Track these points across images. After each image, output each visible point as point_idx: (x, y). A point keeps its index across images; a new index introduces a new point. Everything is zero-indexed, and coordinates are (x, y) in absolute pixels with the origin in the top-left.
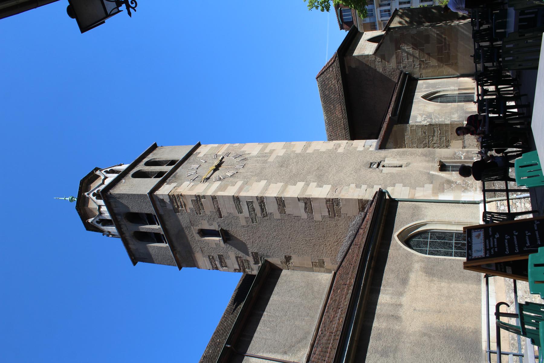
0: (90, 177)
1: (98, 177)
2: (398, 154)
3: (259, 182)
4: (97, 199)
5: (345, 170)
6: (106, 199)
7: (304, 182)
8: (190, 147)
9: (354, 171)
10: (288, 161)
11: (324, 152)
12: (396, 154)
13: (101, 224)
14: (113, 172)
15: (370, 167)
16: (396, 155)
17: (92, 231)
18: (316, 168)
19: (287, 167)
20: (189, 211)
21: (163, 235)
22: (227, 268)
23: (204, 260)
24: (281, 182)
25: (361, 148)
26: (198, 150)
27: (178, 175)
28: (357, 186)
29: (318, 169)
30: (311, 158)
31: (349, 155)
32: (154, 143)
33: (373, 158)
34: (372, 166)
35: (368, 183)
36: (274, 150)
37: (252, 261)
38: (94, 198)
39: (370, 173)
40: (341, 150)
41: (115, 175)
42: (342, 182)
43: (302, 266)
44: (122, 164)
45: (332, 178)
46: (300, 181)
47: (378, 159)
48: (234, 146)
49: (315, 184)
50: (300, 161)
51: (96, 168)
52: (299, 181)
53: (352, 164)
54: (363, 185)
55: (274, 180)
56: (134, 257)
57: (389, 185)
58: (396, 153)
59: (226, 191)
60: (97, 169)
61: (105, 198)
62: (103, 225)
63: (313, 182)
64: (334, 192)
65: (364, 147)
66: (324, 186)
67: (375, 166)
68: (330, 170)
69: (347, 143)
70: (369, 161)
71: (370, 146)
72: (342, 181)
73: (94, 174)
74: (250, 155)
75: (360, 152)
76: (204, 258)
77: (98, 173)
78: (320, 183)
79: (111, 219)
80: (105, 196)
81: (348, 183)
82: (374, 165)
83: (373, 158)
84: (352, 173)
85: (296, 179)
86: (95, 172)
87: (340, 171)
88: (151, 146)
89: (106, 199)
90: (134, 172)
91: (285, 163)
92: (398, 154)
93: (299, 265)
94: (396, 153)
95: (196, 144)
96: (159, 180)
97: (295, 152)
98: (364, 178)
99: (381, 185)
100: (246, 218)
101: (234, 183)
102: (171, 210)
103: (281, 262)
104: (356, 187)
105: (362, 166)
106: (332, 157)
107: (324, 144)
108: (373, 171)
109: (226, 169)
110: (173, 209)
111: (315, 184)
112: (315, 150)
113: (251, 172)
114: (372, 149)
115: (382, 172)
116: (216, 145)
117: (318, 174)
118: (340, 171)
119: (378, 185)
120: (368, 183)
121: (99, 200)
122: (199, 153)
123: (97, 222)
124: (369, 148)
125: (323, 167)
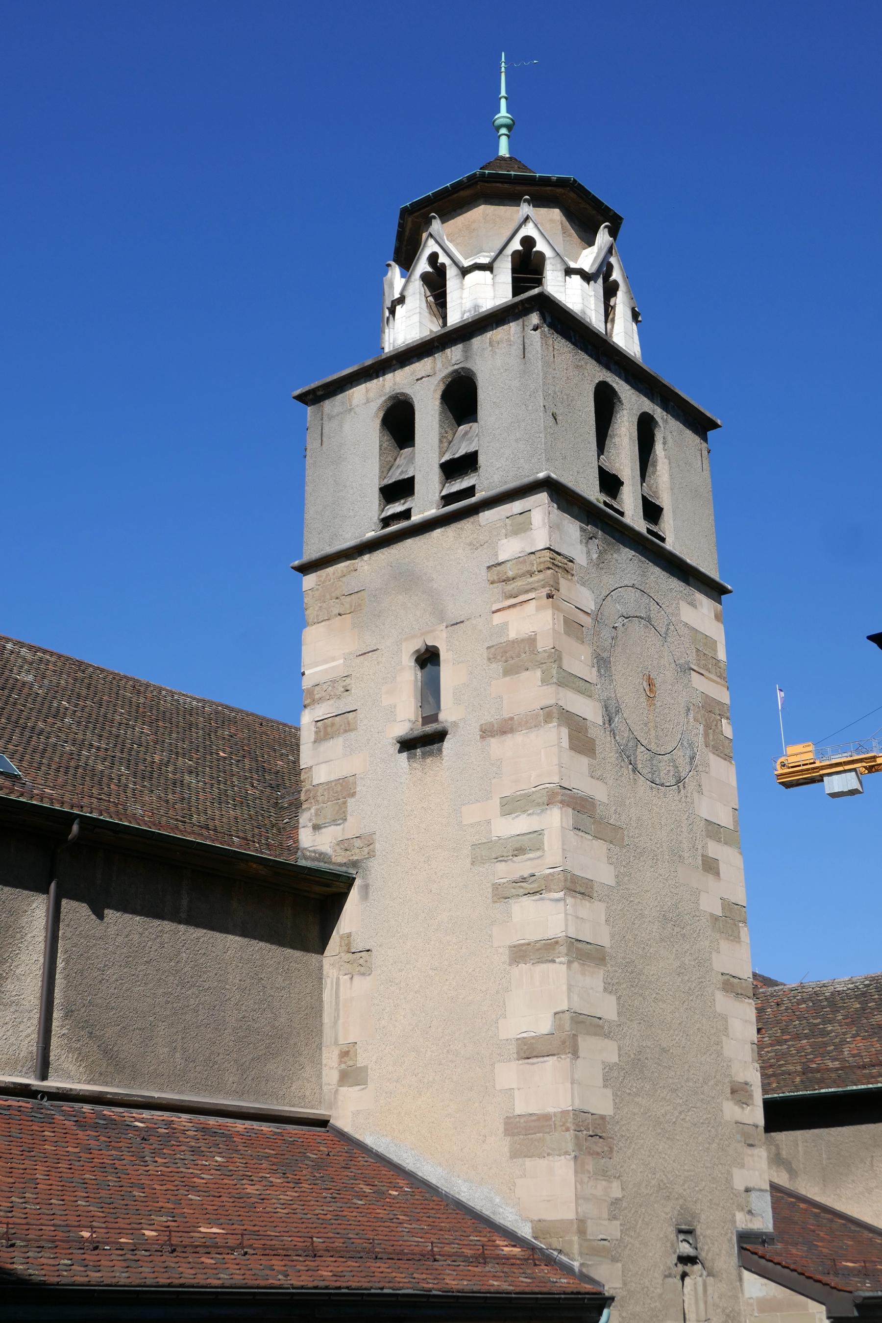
0: (587, 206)
1: (588, 238)
2: (728, 1316)
3: (609, 858)
4: (515, 254)
5: (667, 1146)
6: (517, 311)
7: (616, 1019)
8: (710, 568)
9: (662, 1181)
10: (684, 936)
11: (719, 1054)
12: (727, 1311)
13: (429, 269)
14: (610, 291)
15: (680, 1231)
16: (723, 1311)
17: (401, 226)
18: (664, 1045)
19: (662, 940)
20: (498, 619)
21: (406, 514)
22: (313, 740)
23: (333, 659)
24: (613, 936)
25: (740, 1179)
26: (701, 598)
27: (615, 556)
28: (616, 1202)
29: (664, 1050)
30: (697, 1016)
31: (714, 1145)
32: (719, 422)
33: (709, 1232)
34: (681, 1237)
35: (627, 1238)
36: (717, 874)
37: (343, 829)
38: (516, 245)
39: (661, 1236)
40: (731, 1111)
41: (595, 318)
42: (625, 1150)
43: (341, 1003)
44: (640, 319)
45: (636, 1111)
46: (618, 1004)
47: (709, 1251)
48: (724, 721)
49: (614, 1058)
50: (686, 978)
51: (621, 219)
52: (619, 998)
53: (686, 1167)
54: (621, 1225)
55: (619, 908)
56: (322, 395)
57: (624, 1315)
58: (733, 1310)
59: (573, 753)
60: (613, 232)
61: (520, 307)
62: (425, 277)
63: (620, 1049)
64: (593, 1131)
65: (747, 1190)
66: (609, 1092)
67: (686, 1249)
68: (662, 1095)
69: (757, 1127)
70: (699, 1222)
71: (750, 1212)
72: (629, 1148)
73: (601, 218)
74: (696, 795)
75: (729, 1181)
76: (341, 661)
77: (603, 238)
78: (616, 1074)
79: (448, 325)
80: (527, 305)
81: (622, 1170)
82: (689, 1242)
83: (709, 1232)
84: (658, 1176)
85: (625, 986)
86: (606, 227)
87: (659, 1131)
88: (708, 414)
89: (517, 311)
90: (614, 385)
91: (677, 929)
92: (728, 1316)
93: (342, 997)
94: (733, 1310)
95: (722, 582)
96: (592, 492)
97: (714, 953)
98: (643, 1220)
99: (625, 1284)
100: (489, 822)
101: (598, 773)
102: (496, 555)
103: (349, 935)
104: (612, 1204)
105: (681, 1201)
106: (706, 1087)
107: (748, 1047)
108: (669, 1244)
109: (646, 725)
110: (501, 558)
111: (614, 1058)
112: (724, 1018)
113: (639, 819)
114: (742, 1222)
115: (666, 1276)
116: (722, 655)
117: (647, 1059)
118: (659, 1131)
119: (623, 1276)
120: (627, 1238)
121: (509, 266)
122: (692, 604)
123: (433, 258)
124: (743, 1209)
125: (670, 1068)
